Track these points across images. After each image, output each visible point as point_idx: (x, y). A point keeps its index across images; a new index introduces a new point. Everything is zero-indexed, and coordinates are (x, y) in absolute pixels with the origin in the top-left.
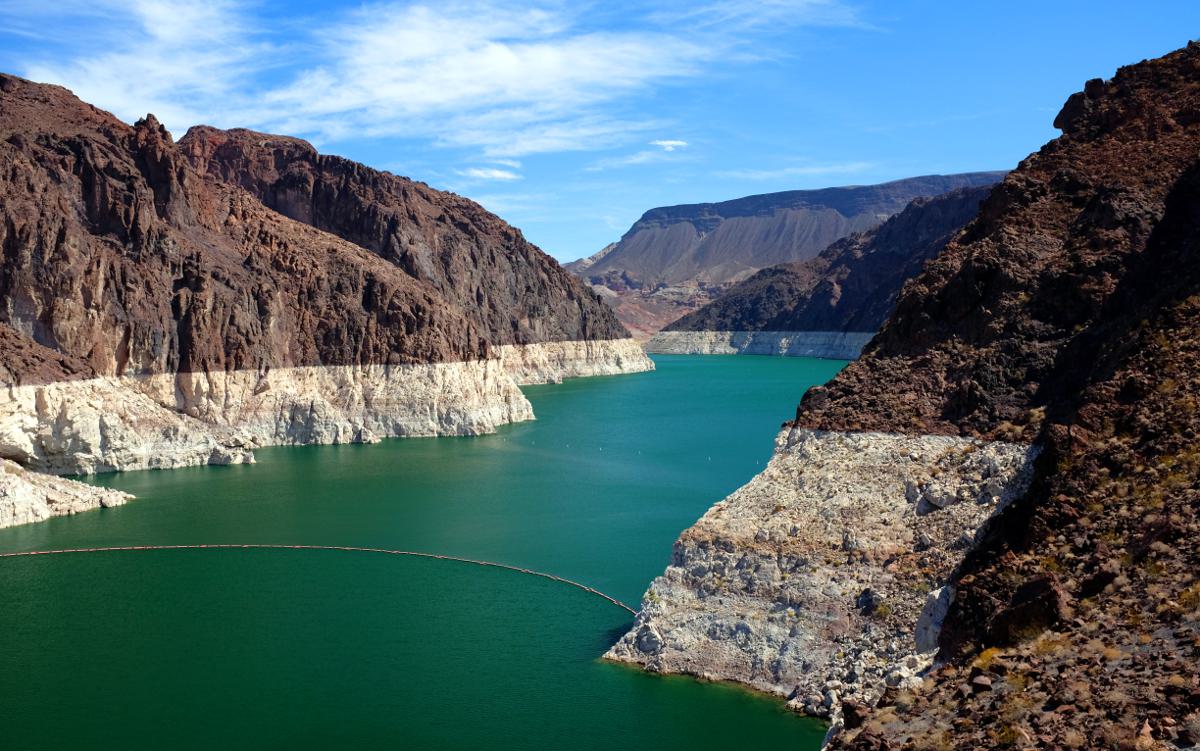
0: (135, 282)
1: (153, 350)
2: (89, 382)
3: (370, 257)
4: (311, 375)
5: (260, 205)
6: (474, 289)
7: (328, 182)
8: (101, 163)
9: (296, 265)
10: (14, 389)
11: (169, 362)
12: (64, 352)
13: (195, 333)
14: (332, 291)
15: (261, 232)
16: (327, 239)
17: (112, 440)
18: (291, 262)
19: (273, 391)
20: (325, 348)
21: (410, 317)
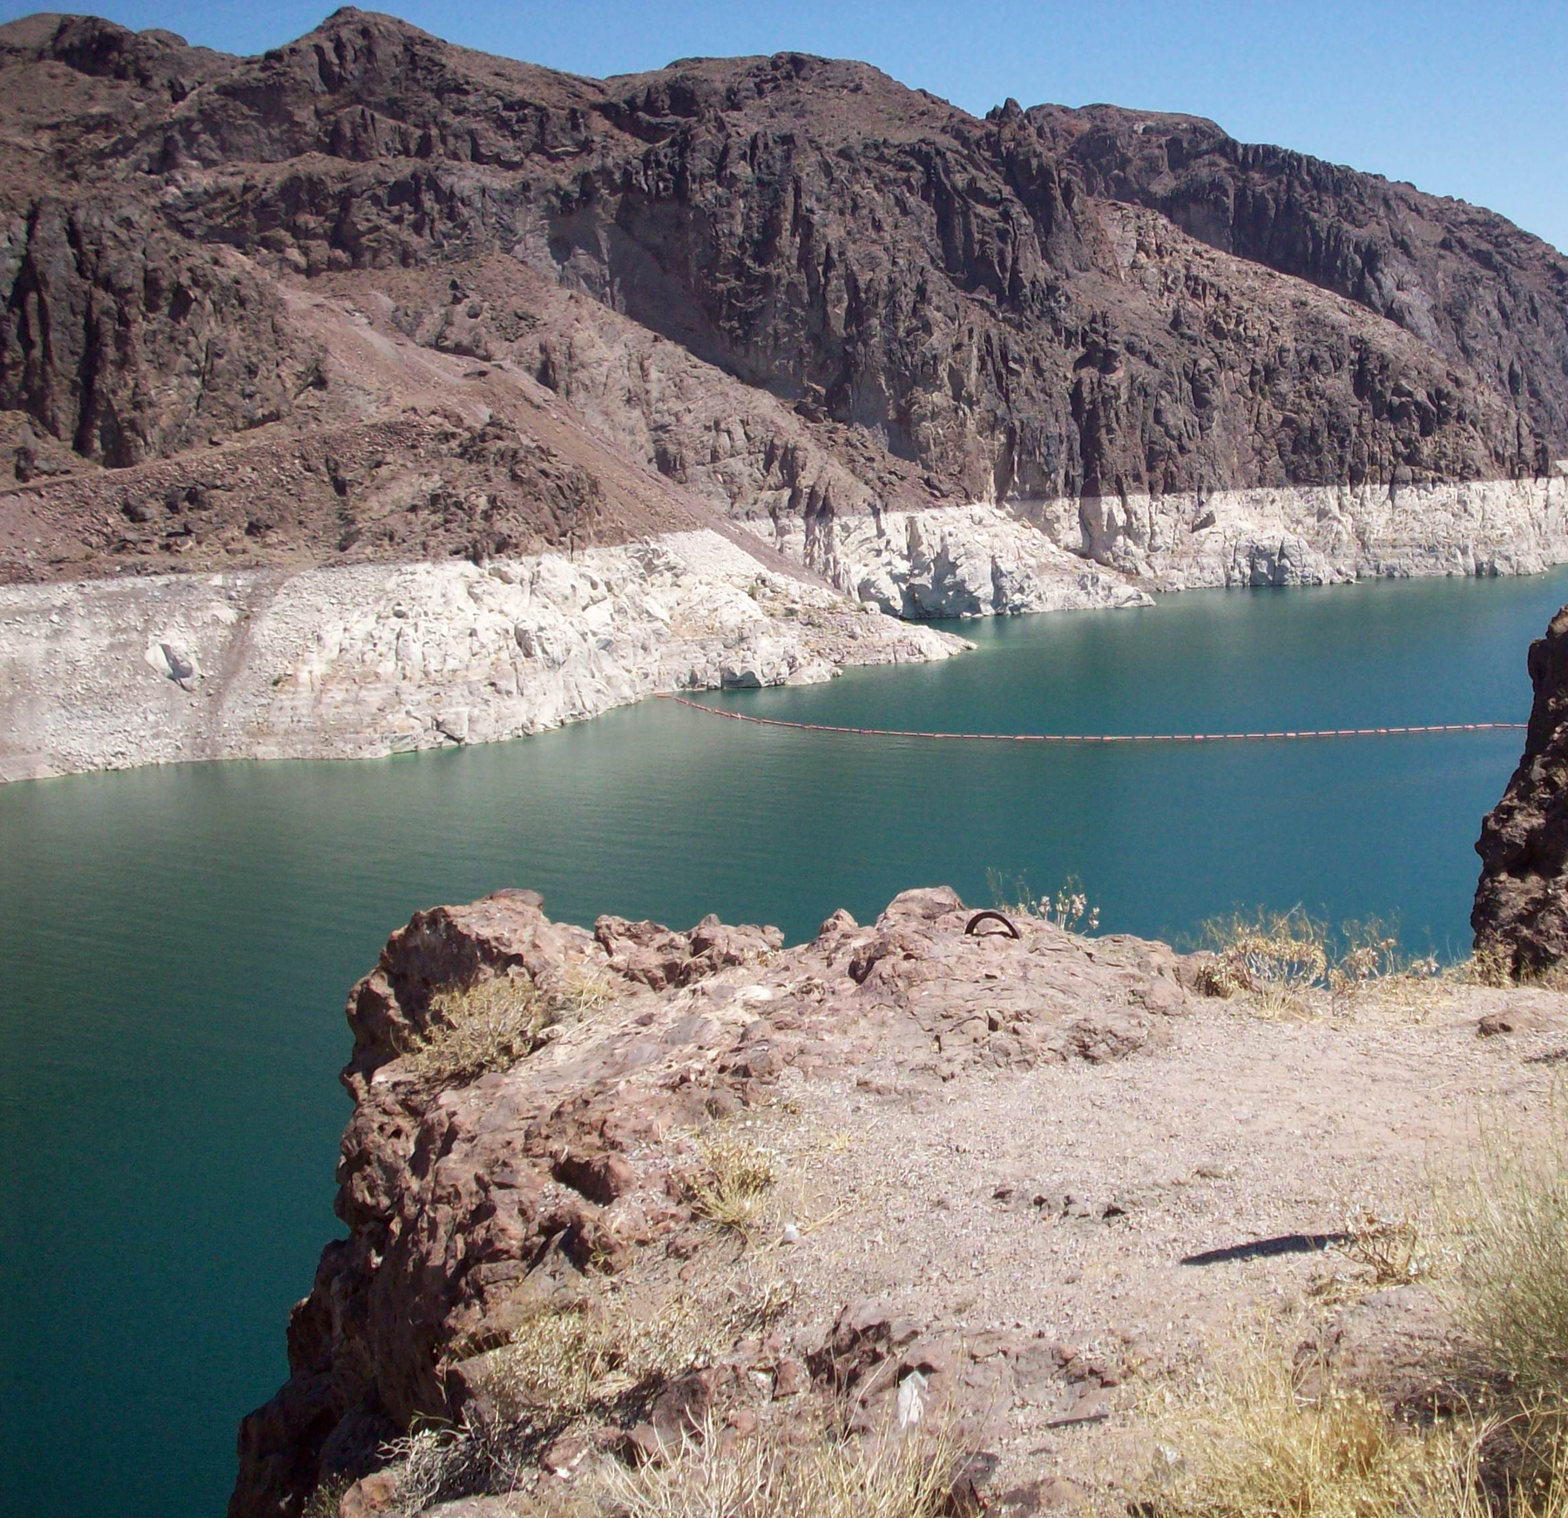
0: (1020, 361)
1: (1047, 463)
2: (966, 509)
3: (1359, 313)
4: (1273, 501)
5: (1182, 235)
6: (1505, 366)
7: (1259, 189)
8: (960, 180)
9: (1245, 329)
10: (882, 516)
11: (1069, 482)
12: (927, 467)
13: (1103, 436)
14: (1302, 370)
15: (1188, 278)
16: (1290, 286)
17: (1009, 593)
18: (1237, 324)
19: (1219, 525)
20: (1294, 458)
21: (1426, 410)
